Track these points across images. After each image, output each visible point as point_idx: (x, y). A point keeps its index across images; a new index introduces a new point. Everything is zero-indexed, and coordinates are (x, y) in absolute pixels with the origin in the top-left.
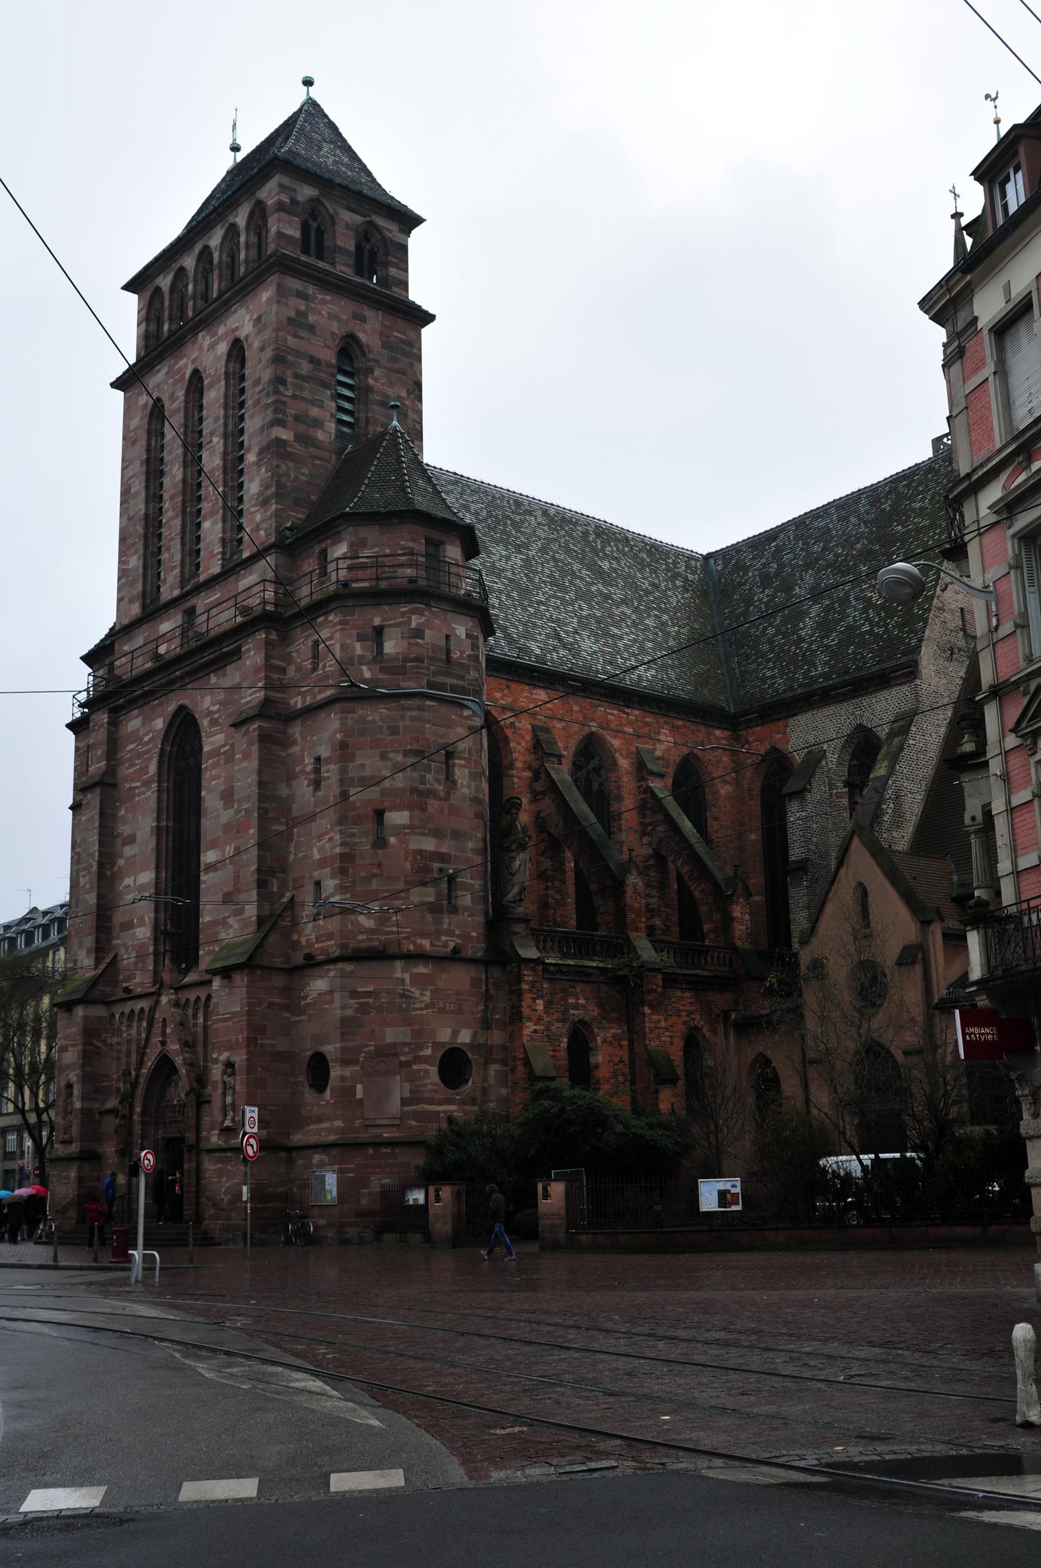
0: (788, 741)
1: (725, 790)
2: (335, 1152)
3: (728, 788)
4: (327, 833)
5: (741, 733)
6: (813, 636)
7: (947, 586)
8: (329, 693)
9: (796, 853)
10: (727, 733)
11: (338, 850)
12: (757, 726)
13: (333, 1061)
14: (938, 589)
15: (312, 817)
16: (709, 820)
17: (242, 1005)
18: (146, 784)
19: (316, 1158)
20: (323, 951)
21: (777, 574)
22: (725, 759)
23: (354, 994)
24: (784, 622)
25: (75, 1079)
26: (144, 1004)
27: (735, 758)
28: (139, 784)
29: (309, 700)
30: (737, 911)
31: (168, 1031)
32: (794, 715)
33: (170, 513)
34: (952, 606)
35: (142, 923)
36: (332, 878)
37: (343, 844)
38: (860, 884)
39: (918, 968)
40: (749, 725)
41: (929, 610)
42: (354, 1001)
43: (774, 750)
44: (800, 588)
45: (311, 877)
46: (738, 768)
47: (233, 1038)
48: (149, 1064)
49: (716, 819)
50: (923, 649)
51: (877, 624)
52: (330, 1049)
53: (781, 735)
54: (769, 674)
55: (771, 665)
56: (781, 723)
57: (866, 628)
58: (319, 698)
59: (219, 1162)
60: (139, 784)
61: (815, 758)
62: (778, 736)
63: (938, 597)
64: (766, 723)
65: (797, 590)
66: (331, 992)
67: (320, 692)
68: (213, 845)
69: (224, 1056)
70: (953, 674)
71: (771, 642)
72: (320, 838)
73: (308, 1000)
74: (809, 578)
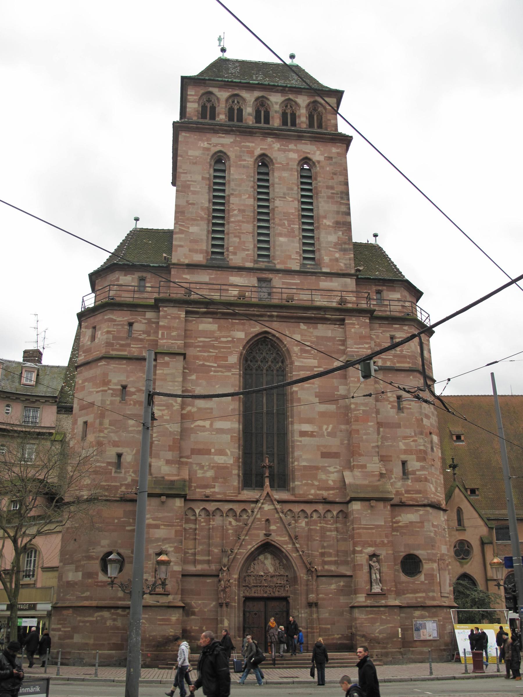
2: (434, 610)
4: (412, 437)
8: (406, 365)
11: (422, 448)
13: (425, 559)
15: (399, 426)
17: (385, 522)
18: (229, 368)
19: (417, 613)
20: (412, 499)
23: (433, 526)
25: (172, 549)
26: (238, 508)
28: (216, 365)
29: (388, 364)
31: (273, 527)
33: (240, 218)
35: (221, 452)
36: (417, 461)
37: (424, 445)
42: (433, 529)
45: (398, 457)
47: (378, 540)
48: (249, 547)
52: (421, 553)
58: (398, 365)
59: (372, 614)
60: (216, 365)
66: (422, 522)
67: (399, 362)
68: (309, 421)
69: (370, 550)
72: (405, 438)
73: (400, 524)
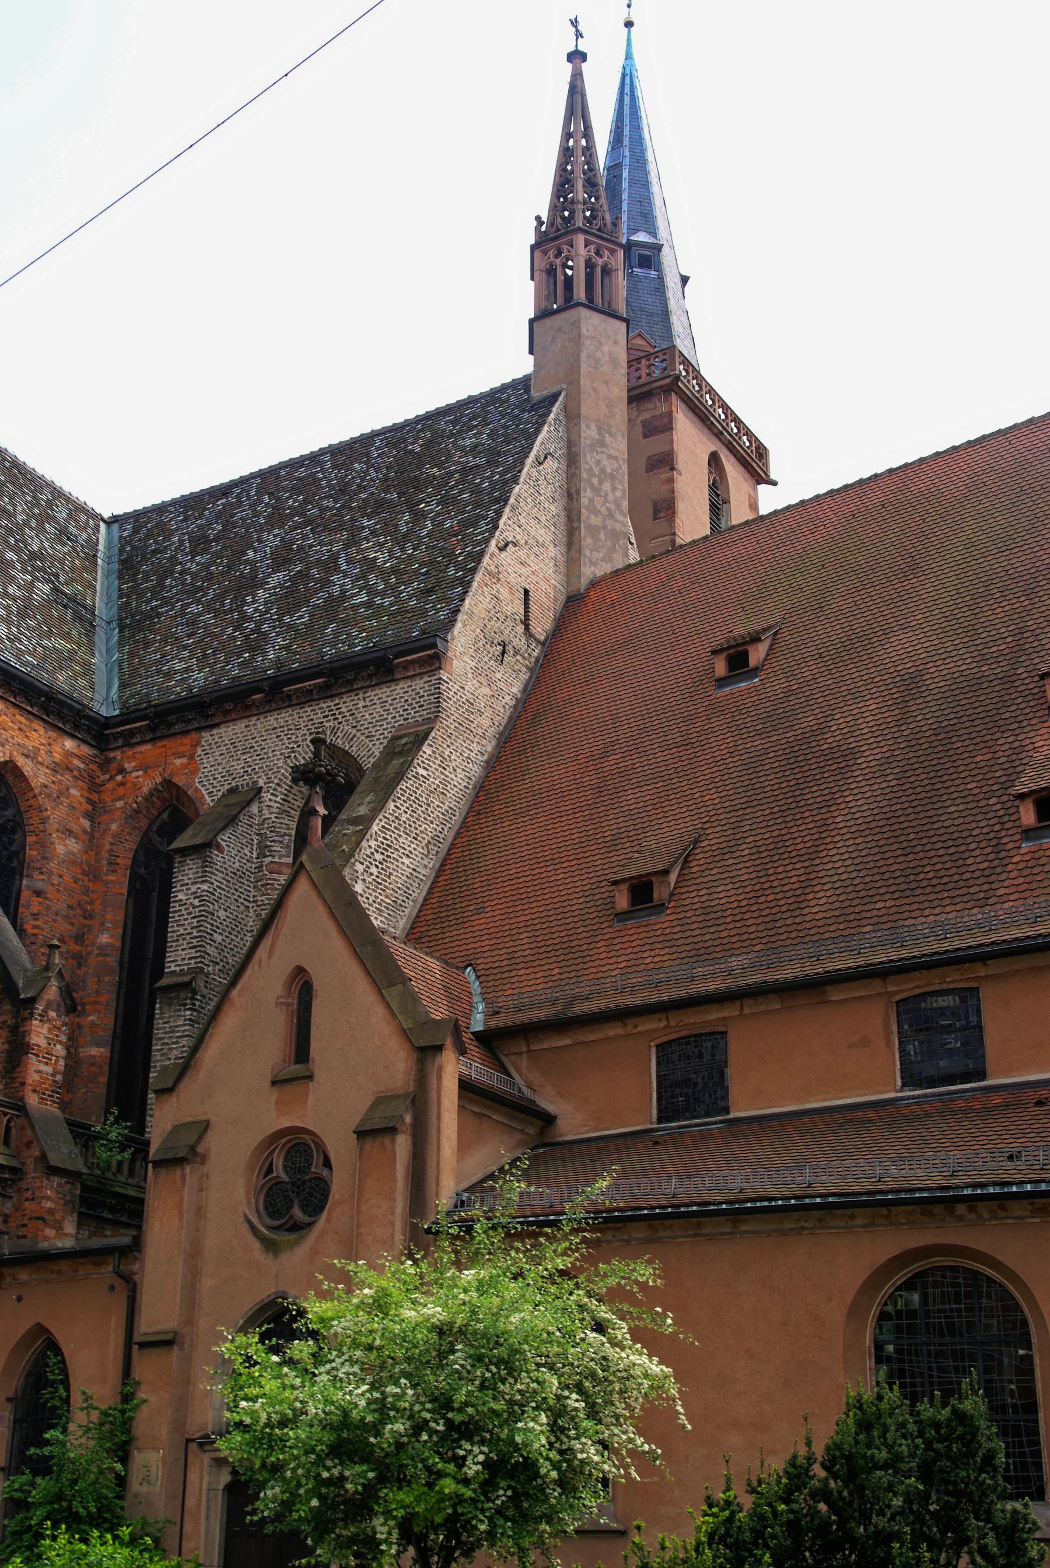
0: (196, 770)
1: (65, 847)
3: (73, 846)
5: (112, 755)
6: (267, 612)
7: (507, 545)
9: (178, 959)
10: (86, 750)
12: (143, 742)
14: (493, 543)
16: (25, 895)
21: (216, 539)
22: (73, 791)
24: (220, 597)
27: (95, 797)
30: (39, 1033)
32: (212, 727)
34: (512, 580)
38: (300, 971)
39: (402, 1144)
40: (129, 740)
41: (474, 570)
43: (168, 783)
44: (255, 551)
46: (95, 812)
49: (38, 893)
50: (459, 625)
51: (383, 594)
53: (185, 760)
54: (179, 666)
55: (186, 654)
56: (187, 740)
57: (363, 598)
61: (240, 800)
62: (178, 762)
63: (492, 555)
64: (160, 738)
65: (251, 553)
70: (502, 685)
71: (193, 622)
74: (272, 539)
